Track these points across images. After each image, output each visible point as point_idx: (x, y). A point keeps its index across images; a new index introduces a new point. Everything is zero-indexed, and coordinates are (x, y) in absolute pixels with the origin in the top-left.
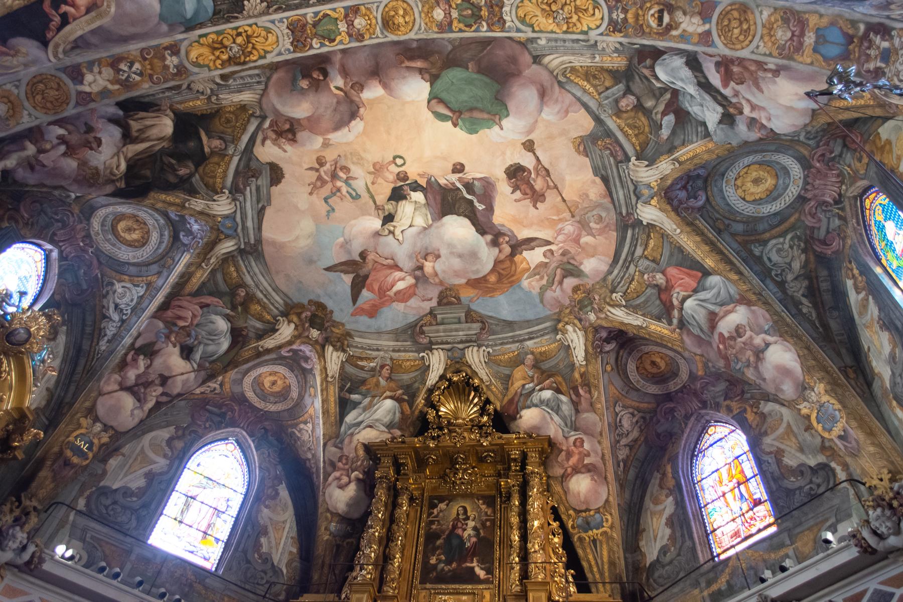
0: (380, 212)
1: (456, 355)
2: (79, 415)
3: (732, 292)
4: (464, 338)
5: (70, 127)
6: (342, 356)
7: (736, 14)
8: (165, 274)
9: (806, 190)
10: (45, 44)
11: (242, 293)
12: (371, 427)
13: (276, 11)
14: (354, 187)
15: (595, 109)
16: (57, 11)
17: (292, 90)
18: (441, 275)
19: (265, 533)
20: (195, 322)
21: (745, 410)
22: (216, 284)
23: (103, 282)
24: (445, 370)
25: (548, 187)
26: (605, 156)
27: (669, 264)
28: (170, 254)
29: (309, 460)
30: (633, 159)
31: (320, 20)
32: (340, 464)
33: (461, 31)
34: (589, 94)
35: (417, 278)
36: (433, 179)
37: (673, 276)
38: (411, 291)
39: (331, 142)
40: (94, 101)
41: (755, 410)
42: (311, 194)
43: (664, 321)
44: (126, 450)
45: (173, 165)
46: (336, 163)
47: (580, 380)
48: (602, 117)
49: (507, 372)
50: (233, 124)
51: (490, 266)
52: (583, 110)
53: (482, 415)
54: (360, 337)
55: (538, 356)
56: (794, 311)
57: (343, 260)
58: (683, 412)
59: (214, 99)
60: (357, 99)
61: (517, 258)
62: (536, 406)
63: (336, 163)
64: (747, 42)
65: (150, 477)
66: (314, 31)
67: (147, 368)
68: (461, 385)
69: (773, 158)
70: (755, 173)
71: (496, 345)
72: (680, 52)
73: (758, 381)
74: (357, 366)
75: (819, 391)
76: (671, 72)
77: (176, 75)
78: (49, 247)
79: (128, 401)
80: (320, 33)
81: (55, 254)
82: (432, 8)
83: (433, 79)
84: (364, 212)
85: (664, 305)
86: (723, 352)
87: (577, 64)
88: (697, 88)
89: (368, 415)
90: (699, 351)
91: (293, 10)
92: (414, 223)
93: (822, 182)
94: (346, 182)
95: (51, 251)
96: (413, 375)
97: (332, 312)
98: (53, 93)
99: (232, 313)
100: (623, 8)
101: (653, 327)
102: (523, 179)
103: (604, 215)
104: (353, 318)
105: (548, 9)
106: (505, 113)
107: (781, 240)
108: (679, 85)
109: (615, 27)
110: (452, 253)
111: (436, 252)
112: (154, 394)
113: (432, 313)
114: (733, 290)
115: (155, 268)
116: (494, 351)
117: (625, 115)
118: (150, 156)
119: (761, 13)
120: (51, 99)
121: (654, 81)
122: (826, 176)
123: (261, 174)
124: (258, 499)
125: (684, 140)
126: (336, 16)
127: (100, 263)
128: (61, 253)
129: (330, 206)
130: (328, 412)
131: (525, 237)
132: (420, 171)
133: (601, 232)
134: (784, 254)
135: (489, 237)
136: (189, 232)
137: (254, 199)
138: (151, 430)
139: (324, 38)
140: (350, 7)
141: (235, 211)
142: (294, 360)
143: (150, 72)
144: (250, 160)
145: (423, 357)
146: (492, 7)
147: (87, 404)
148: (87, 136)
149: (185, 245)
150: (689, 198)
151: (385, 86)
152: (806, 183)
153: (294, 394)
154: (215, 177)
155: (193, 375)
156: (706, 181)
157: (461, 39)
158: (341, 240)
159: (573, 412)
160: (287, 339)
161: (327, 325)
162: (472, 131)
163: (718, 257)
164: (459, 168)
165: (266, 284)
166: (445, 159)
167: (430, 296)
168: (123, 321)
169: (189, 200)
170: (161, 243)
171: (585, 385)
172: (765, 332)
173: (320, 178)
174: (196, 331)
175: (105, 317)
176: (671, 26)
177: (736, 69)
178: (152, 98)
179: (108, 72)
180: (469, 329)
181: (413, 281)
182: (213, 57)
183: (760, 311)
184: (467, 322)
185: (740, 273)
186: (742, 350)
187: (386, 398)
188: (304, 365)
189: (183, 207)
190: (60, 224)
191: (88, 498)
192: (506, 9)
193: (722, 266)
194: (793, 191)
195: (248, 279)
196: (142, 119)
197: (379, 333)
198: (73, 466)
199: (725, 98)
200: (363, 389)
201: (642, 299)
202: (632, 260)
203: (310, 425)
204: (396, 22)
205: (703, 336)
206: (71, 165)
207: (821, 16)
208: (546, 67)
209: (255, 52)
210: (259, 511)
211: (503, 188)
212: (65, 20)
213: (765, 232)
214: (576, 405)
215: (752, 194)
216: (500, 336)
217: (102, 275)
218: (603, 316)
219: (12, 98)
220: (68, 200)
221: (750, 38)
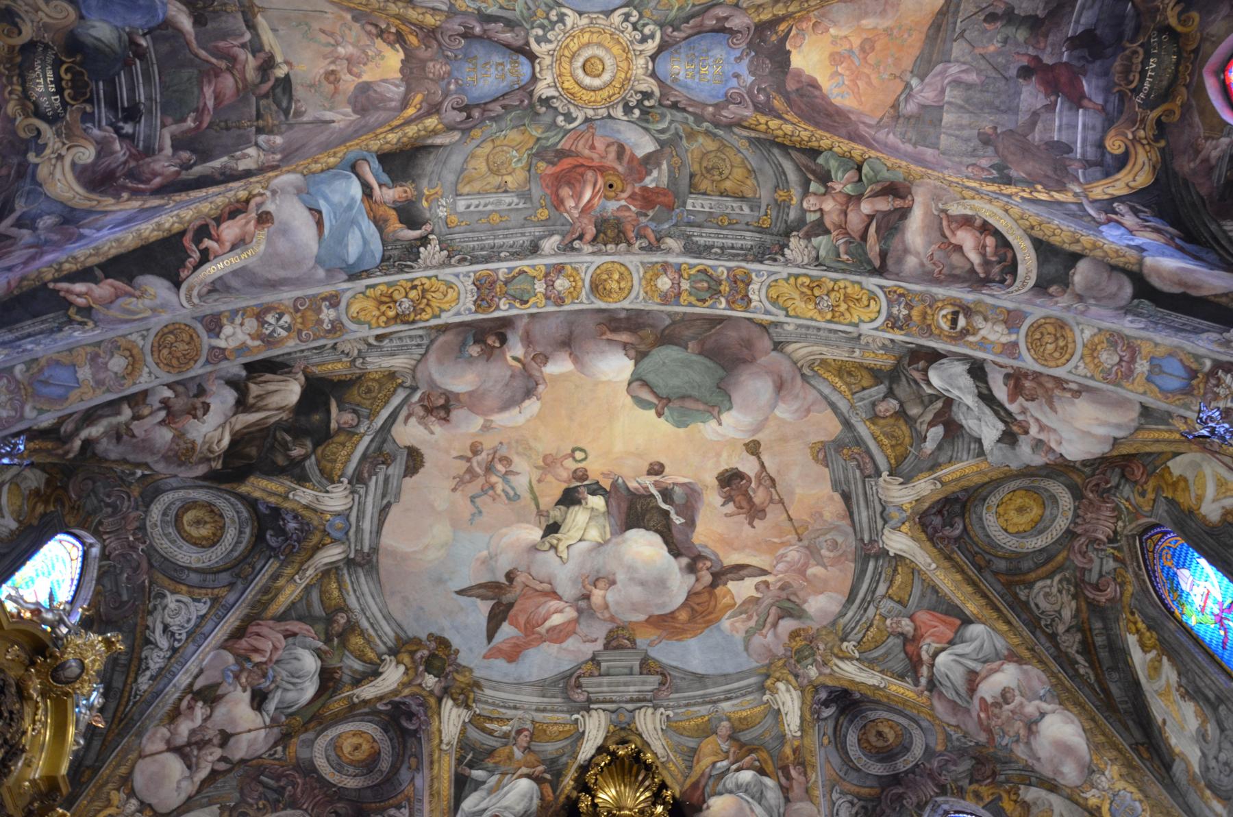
0: (543, 519)
3: (999, 646)
4: (635, 696)
5: (180, 389)
6: (465, 715)
7: (1051, 329)
8: (240, 586)
9: (1076, 524)
10: (177, 284)
11: (342, 619)
13: (460, 261)
14: (513, 485)
16: (197, 246)
17: (457, 358)
18: (612, 609)
20: (275, 658)
21: (1000, 798)
22: (309, 605)
23: (150, 592)
24: (606, 738)
25: (771, 501)
28: (249, 560)
30: (885, 474)
31: (514, 277)
33: (690, 305)
35: (580, 611)
36: (620, 481)
38: (570, 628)
39: (493, 425)
40: (226, 359)
41: (1014, 797)
42: (454, 490)
43: (909, 680)
45: (286, 442)
46: (495, 453)
47: (792, 758)
48: (853, 421)
49: (692, 745)
50: (374, 395)
51: (681, 599)
52: (829, 410)
53: (654, 804)
54: (494, 688)
55: (736, 724)
56: (1071, 672)
57: (483, 581)
58: (915, 799)
59: (359, 362)
60: (537, 374)
61: (719, 590)
62: (731, 792)
63: (495, 453)
64: (1063, 360)
66: (505, 289)
67: (205, 720)
68: (629, 763)
69: (1042, 484)
70: (1019, 501)
71: (679, 707)
72: (964, 358)
73: (1030, 762)
74: (484, 730)
75: (1111, 775)
76: (948, 379)
77: (329, 331)
78: (90, 540)
79: (175, 765)
80: (511, 292)
81: (95, 551)
82: (657, 276)
83: (640, 357)
84: (521, 519)
85: (910, 659)
86: (985, 723)
87: (829, 356)
88: (977, 399)
89: (494, 801)
90: (953, 721)
91: (481, 263)
92: (586, 537)
93: (1094, 515)
94: (505, 477)
95: (91, 545)
96: (560, 745)
97: (457, 652)
98: (182, 347)
99: (325, 647)
100: (907, 304)
103: (840, 540)
105: (809, 292)
106: (728, 405)
107: (1048, 582)
108: (954, 393)
109: (894, 323)
110: (632, 579)
111: (611, 577)
113: (593, 659)
114: (1000, 643)
115: (225, 577)
116: (676, 714)
117: (882, 421)
119: (1082, 331)
120: (179, 354)
121: (924, 386)
122: (1099, 509)
125: (951, 458)
126: (535, 274)
127: (151, 566)
128: (104, 548)
130: (439, 794)
132: (605, 470)
133: (836, 561)
134: (1053, 600)
135: (684, 561)
136: (281, 532)
137: (379, 492)
139: (515, 298)
140: (554, 265)
141: (351, 508)
143: (299, 326)
144: (384, 441)
146: (735, 282)
147: (123, 770)
148: (196, 400)
149: (273, 549)
150: (944, 526)
151: (576, 360)
152: (1076, 516)
153: (385, 765)
154: (335, 461)
155: (263, 732)
156: (964, 507)
157: (685, 314)
158: (485, 553)
159: (782, 801)
160: (392, 687)
161: (449, 669)
162: (680, 424)
163: (983, 602)
164: (656, 469)
167: (595, 636)
168: (174, 650)
169: (295, 489)
170: (238, 543)
171: (799, 764)
172: (1041, 698)
173: (470, 470)
174: (274, 670)
175: (148, 642)
176: (968, 331)
177: (1027, 384)
179: (251, 324)
180: (644, 683)
182: (377, 313)
183: (1034, 671)
184: (641, 674)
185: (1008, 623)
186: (1010, 720)
187: (521, 776)
188: (405, 724)
189: (286, 498)
190: (110, 510)
192: (754, 287)
193: (988, 613)
194: (1062, 524)
195: (352, 601)
196: (265, 382)
197: (519, 684)
199: (1009, 414)
200: (490, 763)
201: (881, 651)
204: (608, 287)
205: (959, 702)
206: (165, 435)
207: (1156, 345)
208: (789, 356)
209: (428, 310)
211: (713, 498)
212: (205, 257)
213: (1030, 571)
214: (785, 790)
215: (1015, 524)
217: (151, 583)
219: (135, 351)
220: (130, 479)
221: (1067, 356)
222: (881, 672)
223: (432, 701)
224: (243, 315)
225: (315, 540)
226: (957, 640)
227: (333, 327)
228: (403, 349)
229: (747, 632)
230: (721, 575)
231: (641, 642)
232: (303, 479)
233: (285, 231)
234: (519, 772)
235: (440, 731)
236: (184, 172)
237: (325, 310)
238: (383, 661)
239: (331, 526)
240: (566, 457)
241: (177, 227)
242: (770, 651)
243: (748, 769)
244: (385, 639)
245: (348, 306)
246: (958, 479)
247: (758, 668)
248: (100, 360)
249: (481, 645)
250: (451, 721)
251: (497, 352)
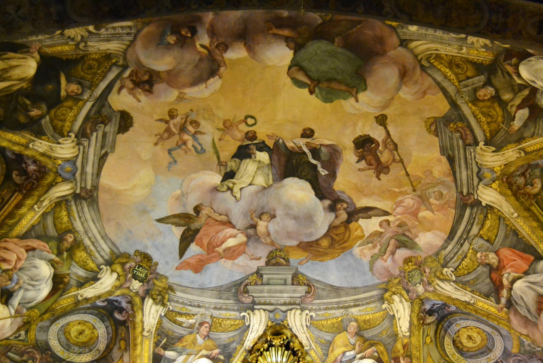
0: (222, 168)
1: (278, 317)
6: (161, 310)
11: (70, 238)
14: (201, 142)
15: (453, 94)
17: (158, 45)
18: (273, 236)
20: (19, 266)
22: (45, 228)
25: (394, 160)
26: (454, 137)
27: (503, 245)
30: (481, 144)
34: (450, 80)
35: (248, 237)
36: (281, 141)
37: (506, 257)
38: (241, 249)
39: (186, 97)
42: (156, 144)
43: (492, 299)
45: (27, 105)
46: (187, 117)
47: (402, 351)
48: (459, 102)
49: (328, 337)
50: (94, 71)
51: (323, 230)
54: (183, 292)
55: (362, 324)
57: (177, 212)
59: (82, 45)
60: (219, 58)
61: (352, 225)
63: (187, 117)
71: (320, 310)
74: (175, 322)
83: (297, 48)
84: (206, 167)
87: (442, 52)
90: (524, 332)
92: (254, 182)
94: (194, 136)
96: (231, 334)
97: (157, 264)
99: (57, 259)
101: (480, 304)
102: (370, 150)
103: (445, 192)
104: (178, 271)
106: (364, 87)
110: (287, 215)
111: (272, 213)
113: (257, 272)
116: (317, 315)
117: (481, 104)
118: (6, 96)
123: (110, 120)
129: (173, 158)
131: (363, 206)
132: (270, 132)
133: (441, 208)
135: (327, 202)
136: (24, 172)
137: (99, 144)
144: (103, 106)
145: (244, 316)
150: (526, 185)
151: (250, 49)
154: (65, 120)
155: (9, 321)
158: (179, 192)
161: (150, 277)
162: (327, 99)
164: (308, 133)
165: (95, 231)
166: (295, 123)
169: (33, 141)
171: (407, 356)
173: (168, 130)
174: (18, 275)
180: (294, 291)
181: (244, 239)
184: (293, 284)
187: (202, 356)
188: (117, 316)
189: (27, 147)
196: (8, 59)
197: (202, 289)
200: (179, 346)
201: (473, 276)
202: (467, 238)
205: (530, 317)
208: (412, 51)
211: (349, 157)
216: (326, 301)
218: (431, 289)
222: (472, 292)
223: (137, 300)
225: (49, 179)
226: (531, 271)
229: (372, 257)
230: (354, 214)
231: (294, 260)
232: (39, 133)
234: (201, 354)
235: (143, 322)
238: (100, 269)
239: (62, 168)
240: (240, 122)
242: (389, 271)
243: (369, 358)
244: (103, 253)
246: (538, 150)
247: (379, 284)
250: (150, 315)
251: (189, 40)
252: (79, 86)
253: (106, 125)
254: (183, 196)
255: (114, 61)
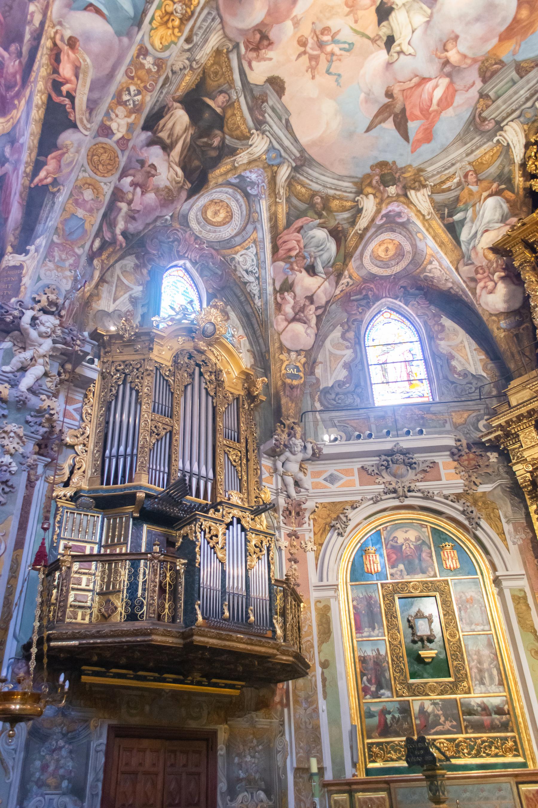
2: (277, 355)
6: (426, 192)
10: (74, 126)
12: (486, 231)
14: (343, 40)
16: (62, 96)
19: (453, 357)
29: (451, 288)
32: (479, 276)
40: (128, 140)
42: (313, 77)
44: (320, 358)
57: (375, 112)
59: (194, 65)
65: (347, 366)
67: (295, 297)
74: (444, 191)
79: (298, 327)
89: (478, 224)
97: (394, 163)
98: (105, 157)
104: (415, 154)
112: (311, 312)
120: (108, 162)
123: (266, 95)
124: (431, 338)
130: (443, 243)
137: (276, 119)
138: (326, 337)
142: (390, 222)
143: (142, 85)
144: (251, 91)
147: (277, 345)
155: (326, 283)
158: (362, 95)
160: (374, 210)
173: (312, 58)
178: (158, 104)
179: (121, 111)
181: (446, 81)
187: (485, 199)
191: (320, 400)
197: (445, 150)
198: (297, 387)
200: (461, 205)
203: (435, 263)
210: (437, 346)
212: (71, 97)
219: (89, 181)
224: (112, 110)
227: (158, 66)
228: (207, 32)
233: (88, 38)
236: (22, 59)
237: (144, 62)
238: (357, 202)
241: (44, 97)
245: (153, 45)
248: (80, 201)
249: (405, 147)
252: (223, 94)
253: (267, 101)
254: (369, 95)
255: (225, 51)
